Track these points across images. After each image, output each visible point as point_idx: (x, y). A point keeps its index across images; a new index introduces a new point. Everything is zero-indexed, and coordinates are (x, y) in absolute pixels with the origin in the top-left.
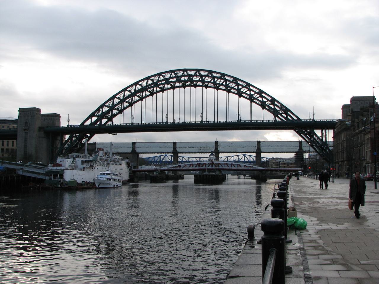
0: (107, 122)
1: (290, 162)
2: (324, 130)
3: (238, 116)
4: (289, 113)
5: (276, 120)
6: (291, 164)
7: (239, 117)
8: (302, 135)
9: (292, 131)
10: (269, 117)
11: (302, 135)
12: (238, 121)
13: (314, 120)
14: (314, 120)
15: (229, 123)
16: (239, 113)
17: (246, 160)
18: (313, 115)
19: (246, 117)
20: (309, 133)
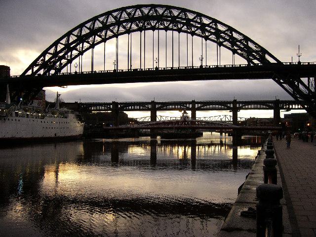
0: (56, 73)
1: (267, 121)
2: (311, 78)
3: (202, 60)
4: (267, 57)
5: (249, 64)
6: (268, 123)
7: (204, 60)
8: (284, 85)
9: (271, 80)
10: (241, 61)
11: (284, 85)
12: (201, 66)
13: (299, 63)
14: (299, 63)
15: (145, 71)
16: (204, 56)
17: (227, 120)
18: (299, 56)
19: (211, 63)
20: (291, 85)
